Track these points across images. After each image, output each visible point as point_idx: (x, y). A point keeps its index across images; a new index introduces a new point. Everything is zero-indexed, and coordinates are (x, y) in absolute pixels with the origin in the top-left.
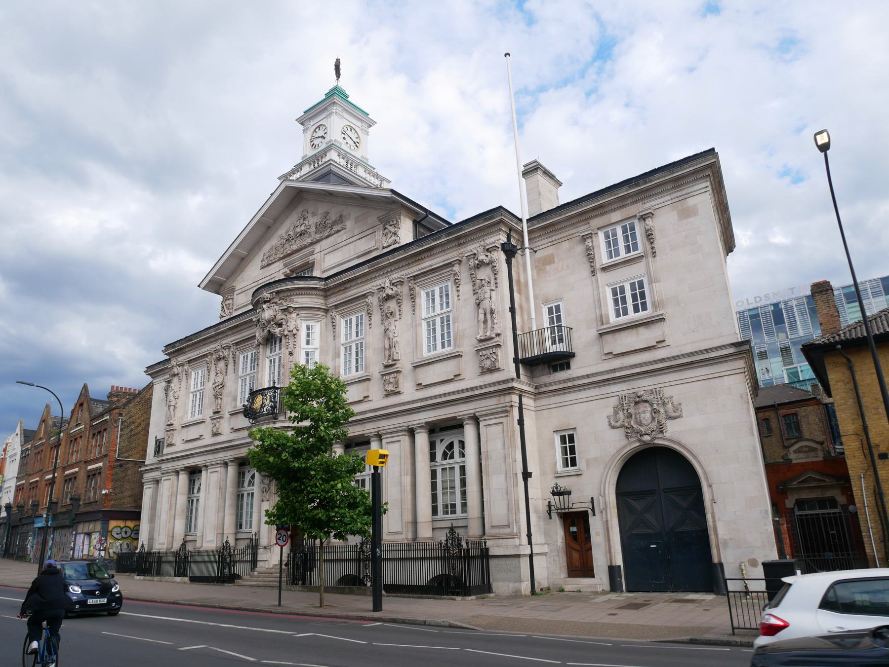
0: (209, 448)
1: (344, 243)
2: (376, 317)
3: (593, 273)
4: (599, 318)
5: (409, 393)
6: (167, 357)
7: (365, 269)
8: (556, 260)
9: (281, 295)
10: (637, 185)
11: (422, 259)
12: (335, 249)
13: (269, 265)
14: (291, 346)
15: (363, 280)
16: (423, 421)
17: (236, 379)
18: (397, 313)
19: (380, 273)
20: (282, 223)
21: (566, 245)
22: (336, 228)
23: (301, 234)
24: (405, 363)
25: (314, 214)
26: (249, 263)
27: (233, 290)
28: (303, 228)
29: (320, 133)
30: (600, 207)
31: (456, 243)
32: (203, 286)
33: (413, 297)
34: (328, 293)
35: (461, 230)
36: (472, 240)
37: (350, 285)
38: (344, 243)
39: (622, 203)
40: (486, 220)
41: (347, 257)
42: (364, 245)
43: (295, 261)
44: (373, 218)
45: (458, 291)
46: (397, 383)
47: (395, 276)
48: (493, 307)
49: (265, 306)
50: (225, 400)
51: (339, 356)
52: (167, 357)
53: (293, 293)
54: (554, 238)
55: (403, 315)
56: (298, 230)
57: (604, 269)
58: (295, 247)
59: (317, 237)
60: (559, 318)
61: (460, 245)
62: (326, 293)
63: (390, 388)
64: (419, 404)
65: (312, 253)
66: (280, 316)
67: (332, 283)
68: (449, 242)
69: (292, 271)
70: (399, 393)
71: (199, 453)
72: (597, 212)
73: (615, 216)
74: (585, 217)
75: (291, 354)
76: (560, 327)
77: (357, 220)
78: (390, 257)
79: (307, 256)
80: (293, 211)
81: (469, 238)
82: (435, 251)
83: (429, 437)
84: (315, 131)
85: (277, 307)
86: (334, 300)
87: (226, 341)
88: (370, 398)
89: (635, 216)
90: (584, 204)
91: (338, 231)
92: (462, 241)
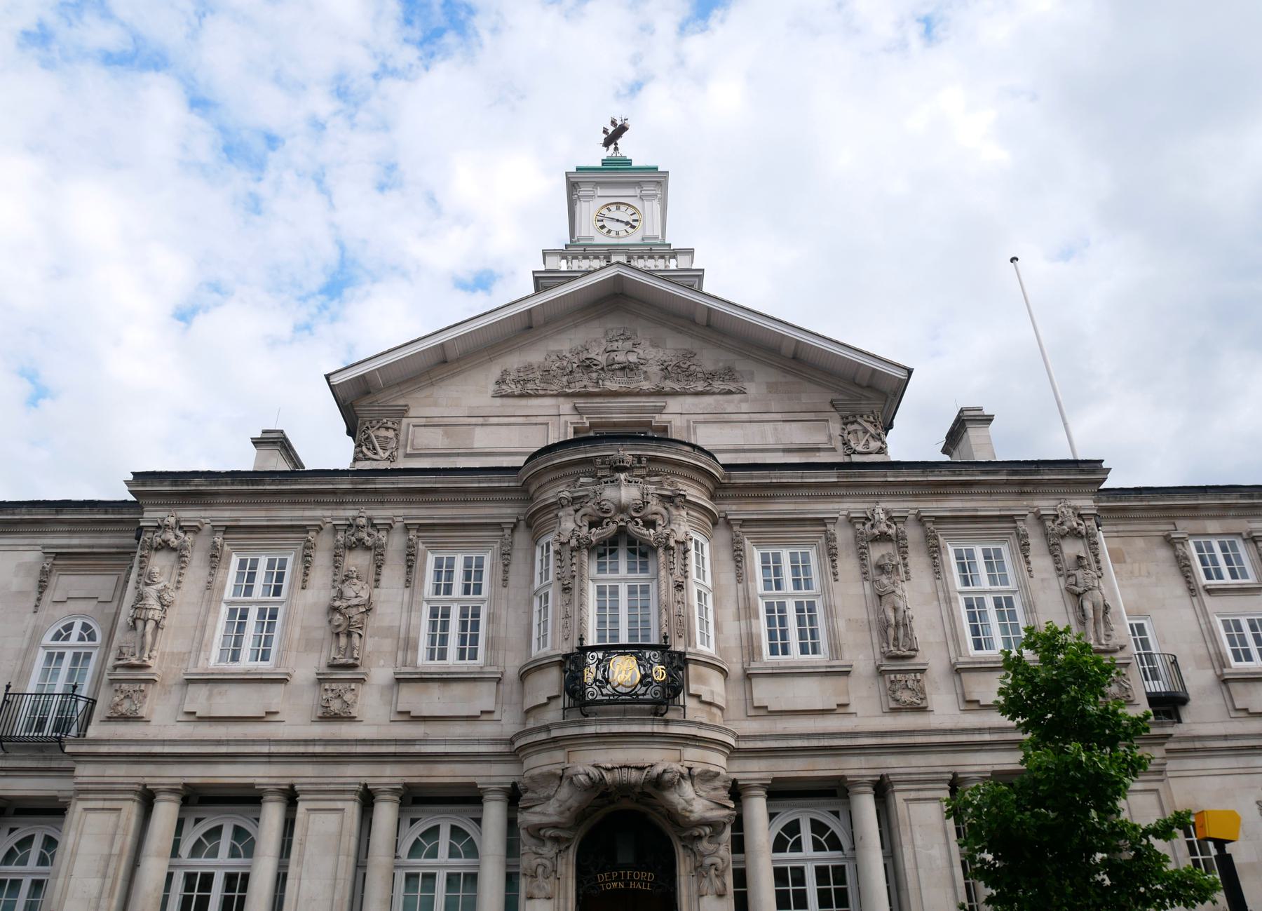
0: (318, 749)
1: (745, 417)
2: (848, 565)
3: (1192, 591)
4: (1214, 657)
5: (944, 711)
6: (132, 498)
7: (831, 477)
8: (1128, 560)
9: (654, 467)
10: (1251, 497)
11: (947, 494)
12: (720, 419)
13: (521, 396)
14: (677, 572)
15: (812, 492)
16: (989, 768)
17: (412, 606)
18: (901, 569)
19: (853, 492)
20: (559, 332)
21: (1140, 543)
22: (718, 385)
23: (626, 368)
24: (933, 656)
25: (655, 345)
26: (453, 375)
27: (403, 412)
28: (633, 358)
29: (624, 215)
30: (1195, 508)
31: (1016, 489)
32: (336, 380)
33: (934, 552)
34: (720, 493)
35: (1037, 472)
36: (1044, 493)
37: (778, 492)
38: (745, 417)
39: (1223, 511)
40: (1082, 472)
41: (757, 442)
42: (798, 434)
43: (610, 410)
44: (817, 397)
45: (1028, 563)
46: (922, 691)
47: (896, 506)
48: (1107, 602)
49: (623, 476)
50: (370, 644)
51: (757, 617)
52: (132, 498)
53: (678, 470)
54: (1121, 528)
55: (912, 574)
56: (620, 358)
57: (1210, 591)
58: (611, 385)
59: (668, 385)
60: (1145, 644)
61: (1021, 493)
62: (719, 490)
63: (906, 696)
64: (987, 737)
65: (660, 410)
66: (654, 505)
67: (740, 478)
68: (1008, 483)
69: (592, 426)
70: (923, 710)
71: (269, 755)
72: (1187, 513)
73: (1213, 526)
74: (1170, 513)
75: (679, 587)
76: (1150, 658)
77: (772, 388)
78: (889, 472)
79: (642, 410)
80: (599, 317)
81: (1040, 489)
82: (975, 489)
83: (509, 810)
84: (607, 206)
85: (652, 489)
86: (734, 509)
87: (381, 514)
88: (851, 710)
89: (1240, 534)
90: (1178, 496)
91: (730, 392)
92: (1028, 489)
